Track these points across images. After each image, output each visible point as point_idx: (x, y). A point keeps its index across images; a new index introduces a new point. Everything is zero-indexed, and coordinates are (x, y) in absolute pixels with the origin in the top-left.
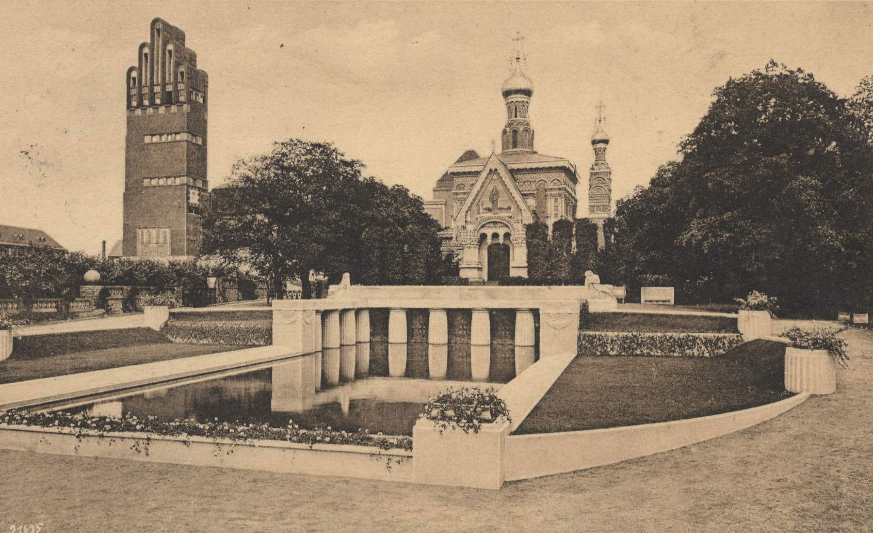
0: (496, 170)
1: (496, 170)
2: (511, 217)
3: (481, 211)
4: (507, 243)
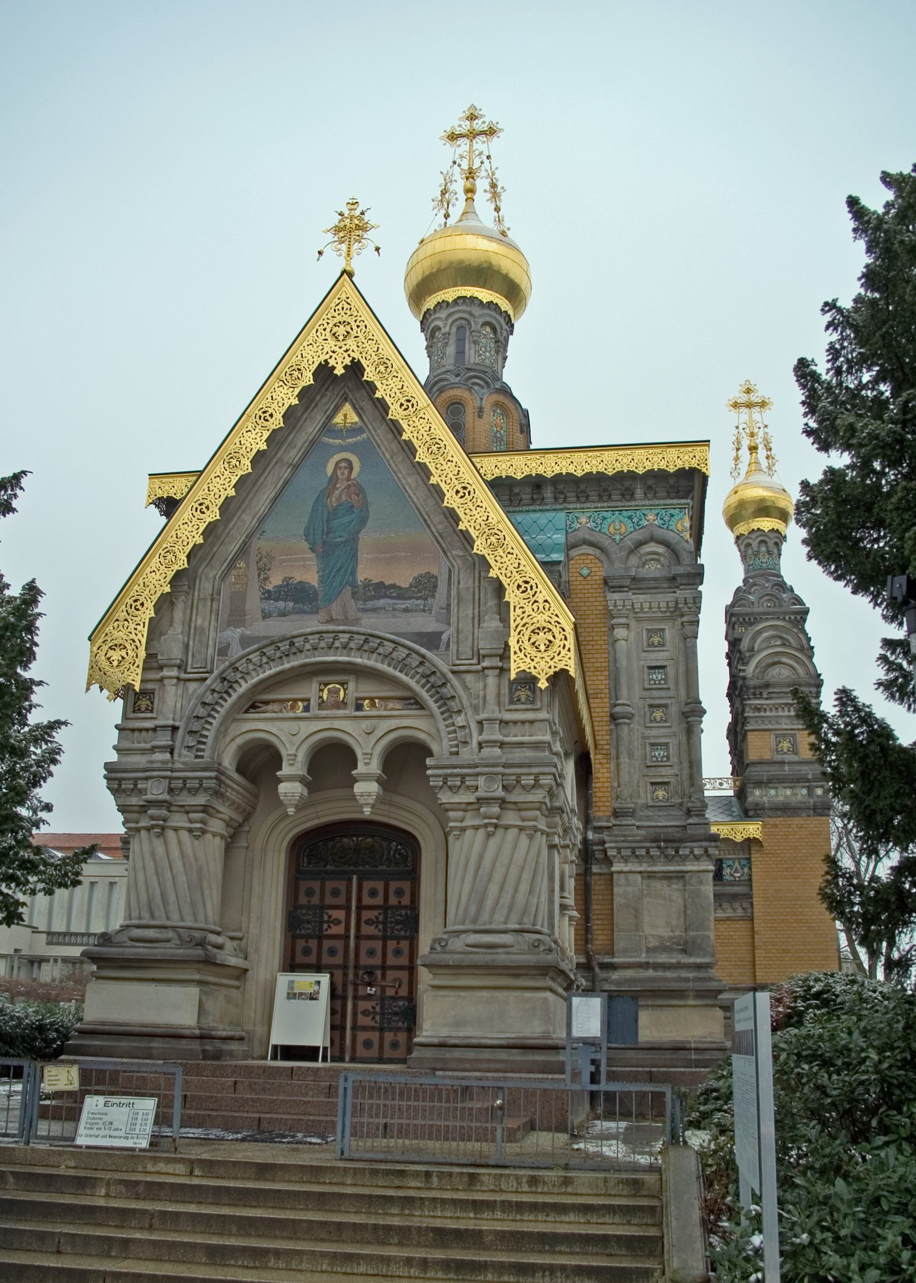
0: (355, 368)
1: (355, 368)
2: (432, 640)
3: (254, 602)
4: (408, 816)
